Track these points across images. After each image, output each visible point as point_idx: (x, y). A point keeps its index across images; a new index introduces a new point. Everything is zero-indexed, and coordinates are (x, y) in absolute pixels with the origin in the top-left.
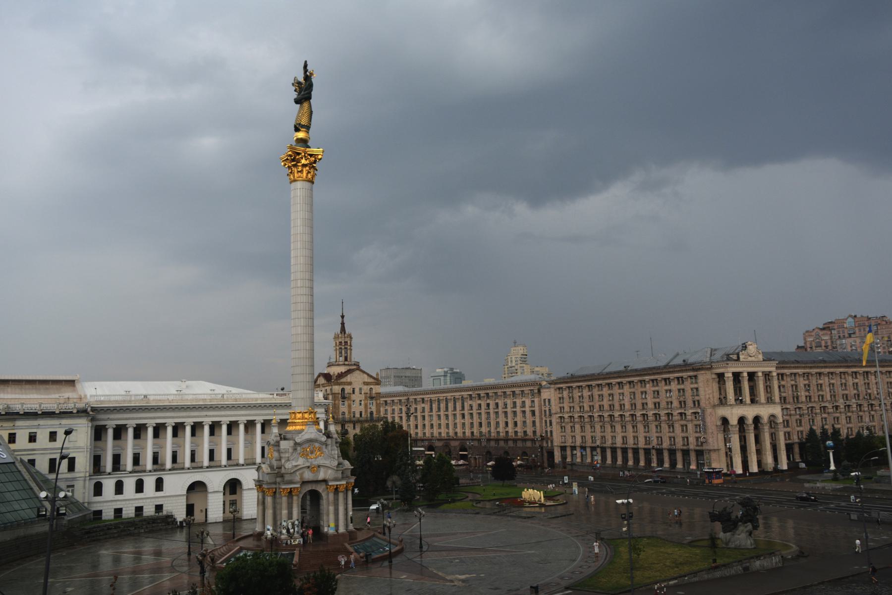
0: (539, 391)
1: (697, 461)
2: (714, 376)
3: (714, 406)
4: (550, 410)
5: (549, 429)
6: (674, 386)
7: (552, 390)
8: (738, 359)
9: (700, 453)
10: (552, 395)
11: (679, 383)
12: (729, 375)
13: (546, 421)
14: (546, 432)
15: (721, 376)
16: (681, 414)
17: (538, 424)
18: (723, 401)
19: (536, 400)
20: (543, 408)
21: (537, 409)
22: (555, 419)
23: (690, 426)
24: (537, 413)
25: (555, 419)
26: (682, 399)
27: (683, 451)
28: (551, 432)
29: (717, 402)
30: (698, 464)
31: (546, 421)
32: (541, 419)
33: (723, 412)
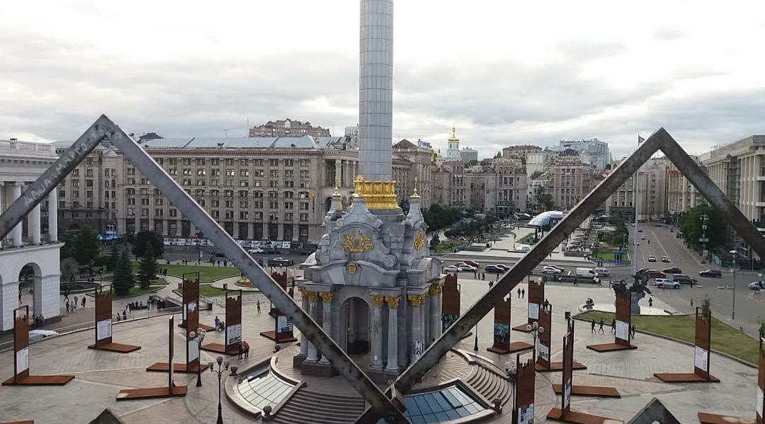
0: (100, 160)
1: (300, 234)
2: (323, 161)
3: (321, 188)
4: (113, 181)
5: (110, 201)
6: (281, 167)
7: (121, 161)
8: (345, 148)
9: (303, 227)
10: (121, 165)
11: (287, 164)
12: (338, 162)
13: (107, 193)
14: (107, 204)
15: (331, 164)
16: (286, 193)
17: (96, 195)
18: (331, 183)
19: (96, 169)
20: (104, 178)
21: (96, 179)
22: (120, 192)
23: (296, 204)
24: (96, 184)
25: (120, 192)
26: (289, 179)
27: (255, 224)
28: (114, 204)
29: (323, 183)
30: (300, 237)
31: (107, 193)
32: (100, 189)
33: (329, 192)
